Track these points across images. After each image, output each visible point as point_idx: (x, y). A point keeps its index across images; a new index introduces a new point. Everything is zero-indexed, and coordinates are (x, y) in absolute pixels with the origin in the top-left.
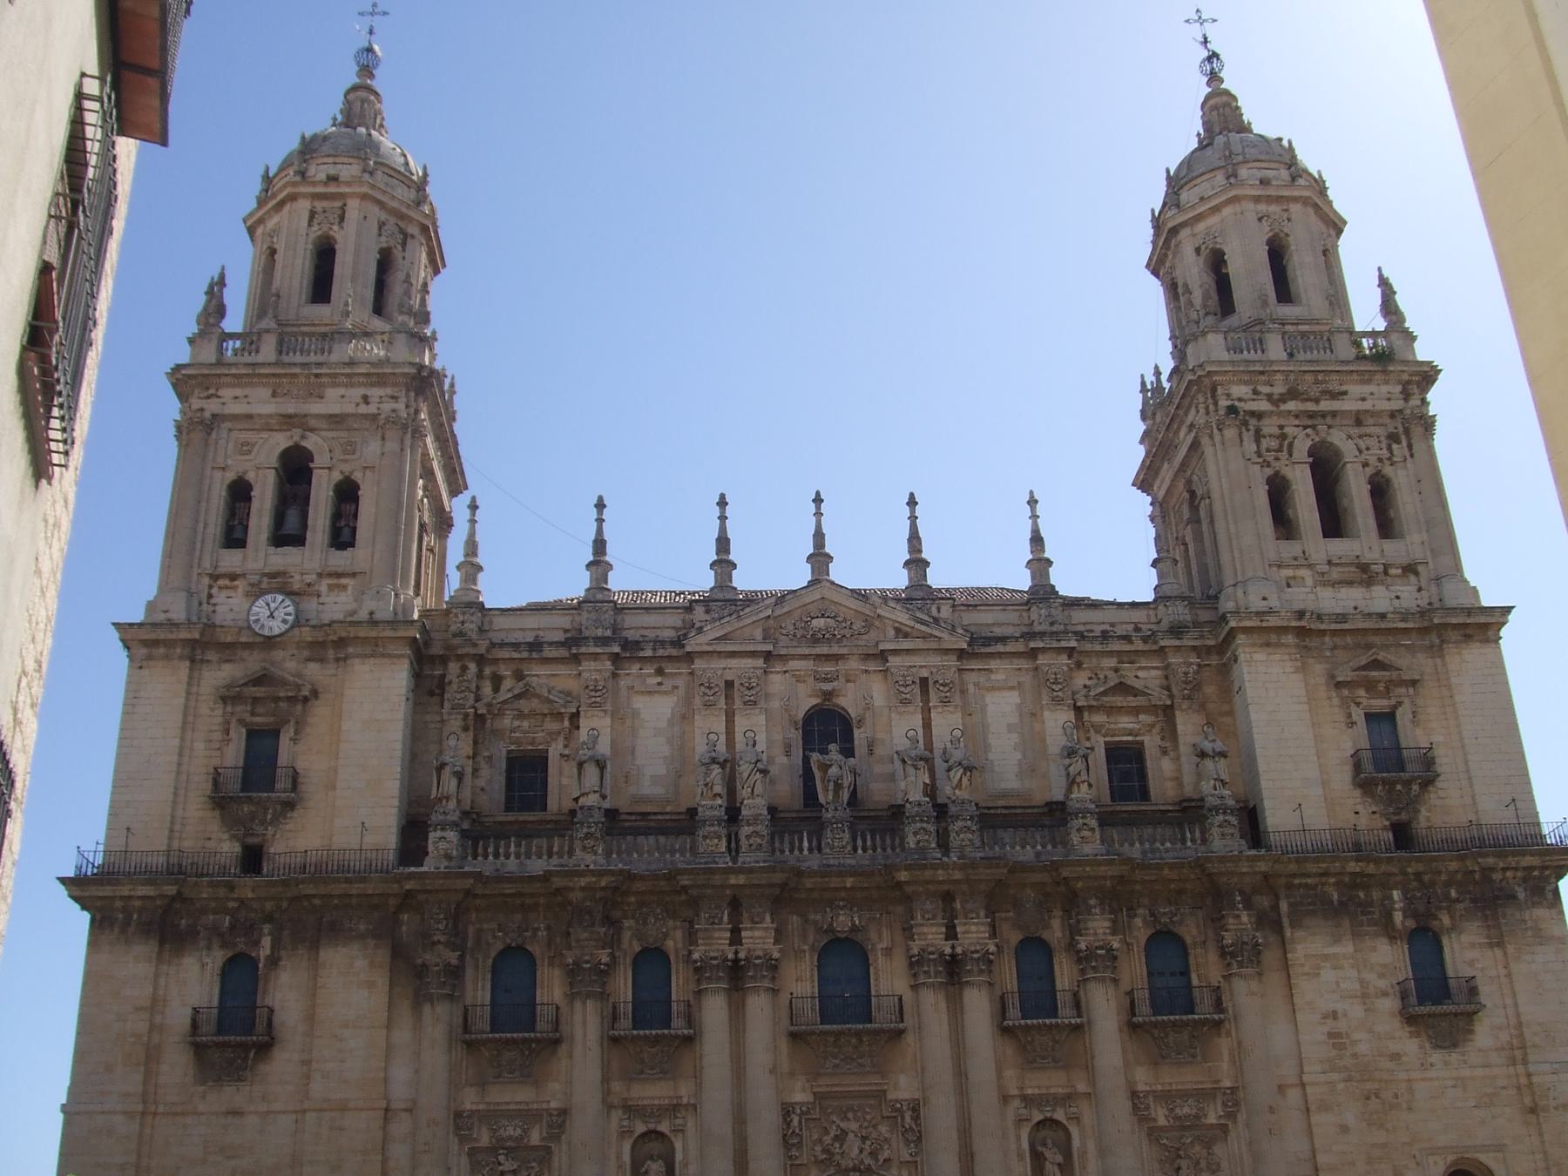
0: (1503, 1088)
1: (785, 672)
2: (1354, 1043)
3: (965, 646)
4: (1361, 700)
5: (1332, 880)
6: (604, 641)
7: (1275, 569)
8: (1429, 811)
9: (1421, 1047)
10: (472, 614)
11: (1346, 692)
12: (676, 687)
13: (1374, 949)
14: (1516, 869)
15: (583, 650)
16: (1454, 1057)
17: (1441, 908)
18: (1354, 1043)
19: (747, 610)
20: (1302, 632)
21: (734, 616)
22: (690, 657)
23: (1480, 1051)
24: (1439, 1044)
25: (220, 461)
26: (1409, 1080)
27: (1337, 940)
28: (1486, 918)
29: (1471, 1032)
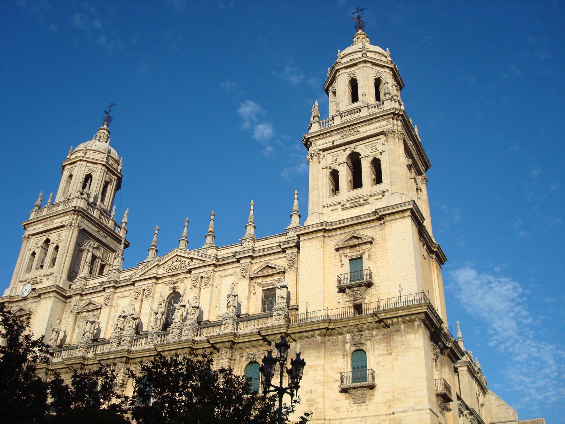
0: (384, 420)
1: (162, 283)
2: (317, 403)
3: (214, 262)
4: (347, 254)
5: (317, 332)
6: (109, 282)
7: (326, 208)
8: (370, 297)
9: (349, 404)
10: (81, 281)
11: (341, 252)
12: (130, 294)
13: (336, 361)
14: (397, 317)
15: (105, 286)
16: (363, 407)
17: (366, 340)
18: (317, 403)
19: (150, 264)
20: (325, 231)
21: (146, 267)
22: (134, 283)
23: (376, 404)
24: (357, 402)
25: (29, 248)
26: (340, 419)
27: (318, 358)
28: (387, 342)
29: (373, 395)
